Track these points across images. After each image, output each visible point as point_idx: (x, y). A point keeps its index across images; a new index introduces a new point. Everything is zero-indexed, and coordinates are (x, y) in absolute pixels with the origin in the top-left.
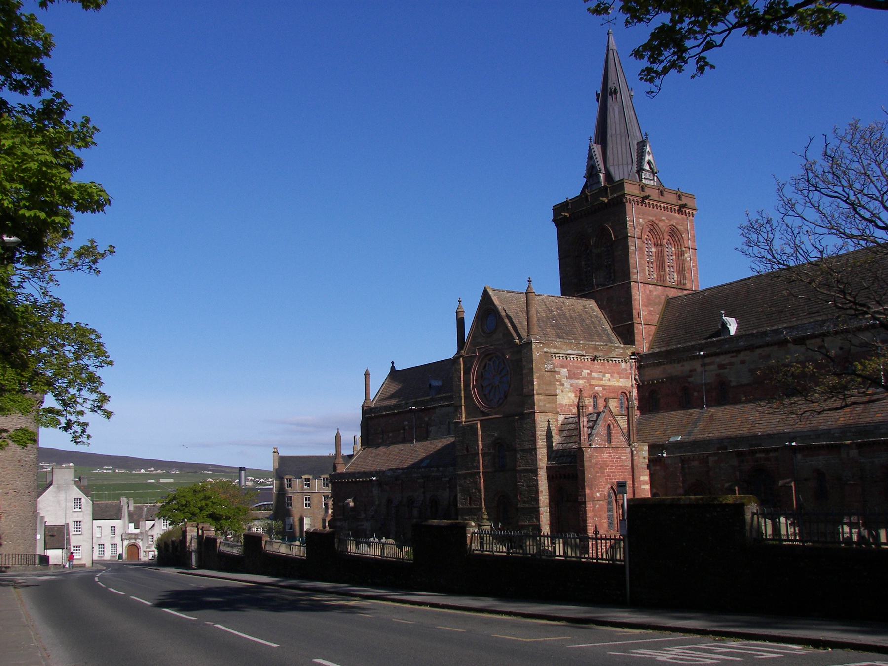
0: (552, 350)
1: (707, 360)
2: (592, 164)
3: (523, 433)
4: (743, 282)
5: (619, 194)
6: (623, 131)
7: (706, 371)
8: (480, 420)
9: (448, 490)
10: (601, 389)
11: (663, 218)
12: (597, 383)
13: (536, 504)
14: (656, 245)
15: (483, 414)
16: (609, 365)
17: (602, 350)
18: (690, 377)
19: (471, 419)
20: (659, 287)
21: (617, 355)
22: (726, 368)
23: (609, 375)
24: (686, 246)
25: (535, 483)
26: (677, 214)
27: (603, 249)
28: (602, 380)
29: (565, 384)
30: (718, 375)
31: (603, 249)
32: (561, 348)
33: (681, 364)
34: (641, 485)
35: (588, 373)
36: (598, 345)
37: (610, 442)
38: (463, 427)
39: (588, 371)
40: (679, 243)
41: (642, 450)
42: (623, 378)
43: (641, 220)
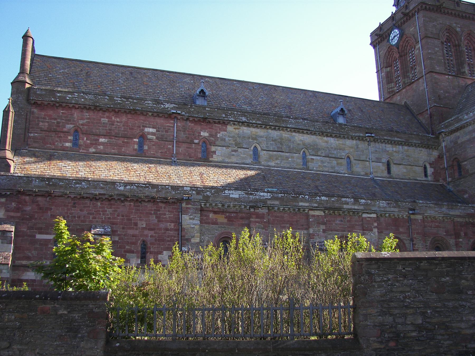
9: (376, 230)
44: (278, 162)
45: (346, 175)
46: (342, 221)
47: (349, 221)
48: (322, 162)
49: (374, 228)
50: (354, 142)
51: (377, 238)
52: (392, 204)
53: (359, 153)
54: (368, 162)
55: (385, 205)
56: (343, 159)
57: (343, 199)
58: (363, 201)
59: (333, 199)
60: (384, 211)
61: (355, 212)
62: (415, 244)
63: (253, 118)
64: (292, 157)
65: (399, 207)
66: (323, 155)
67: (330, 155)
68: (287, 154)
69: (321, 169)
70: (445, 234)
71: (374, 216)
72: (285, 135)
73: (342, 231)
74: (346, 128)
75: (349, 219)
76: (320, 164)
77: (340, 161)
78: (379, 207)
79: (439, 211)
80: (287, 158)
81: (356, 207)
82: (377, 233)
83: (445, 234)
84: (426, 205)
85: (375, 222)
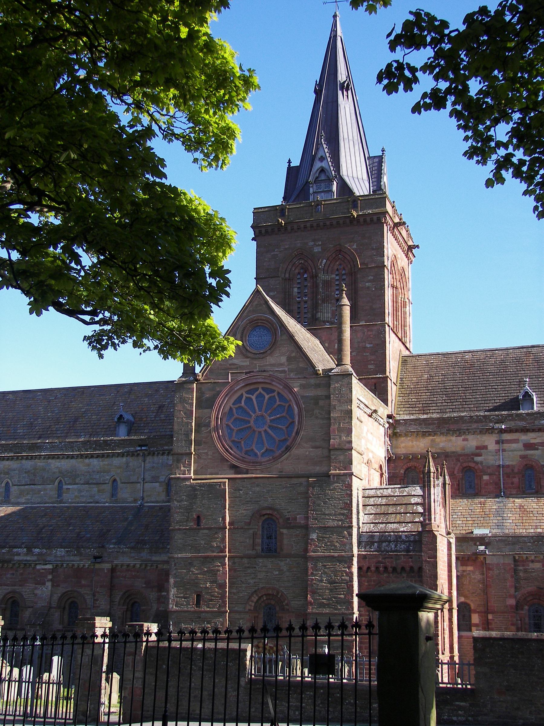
1: (506, 436)
2: (322, 167)
3: (325, 503)
4: (525, 350)
5: (377, 211)
6: (356, 138)
7: (504, 450)
8: (229, 479)
9: (49, 584)
13: (347, 609)
15: (235, 469)
18: (479, 455)
19: (208, 476)
22: (537, 449)
25: (347, 578)
27: (334, 276)
30: (523, 457)
31: (334, 276)
33: (463, 437)
38: (192, 487)
44: (29, 497)
45: (107, 504)
46: (13, 574)
47: (22, 574)
48: (80, 491)
49: (48, 581)
50: (124, 459)
51: (49, 593)
52: (72, 551)
53: (129, 473)
54: (139, 484)
55: (63, 553)
56: (106, 483)
57: (15, 550)
58: (37, 550)
59: (3, 551)
60: (60, 561)
61: (26, 565)
62: (97, 600)
63: (5, 450)
64: (45, 490)
65: (80, 554)
66: (82, 482)
67: (91, 481)
68: (39, 487)
69: (77, 500)
70: (144, 586)
71: (50, 567)
72: (40, 463)
73: (12, 585)
74: (113, 443)
75: (22, 571)
76: (76, 494)
77: (103, 487)
78: (56, 556)
79: (136, 557)
80: (40, 491)
81: (28, 558)
82: (50, 588)
83: (144, 586)
84: (118, 550)
85: (49, 574)
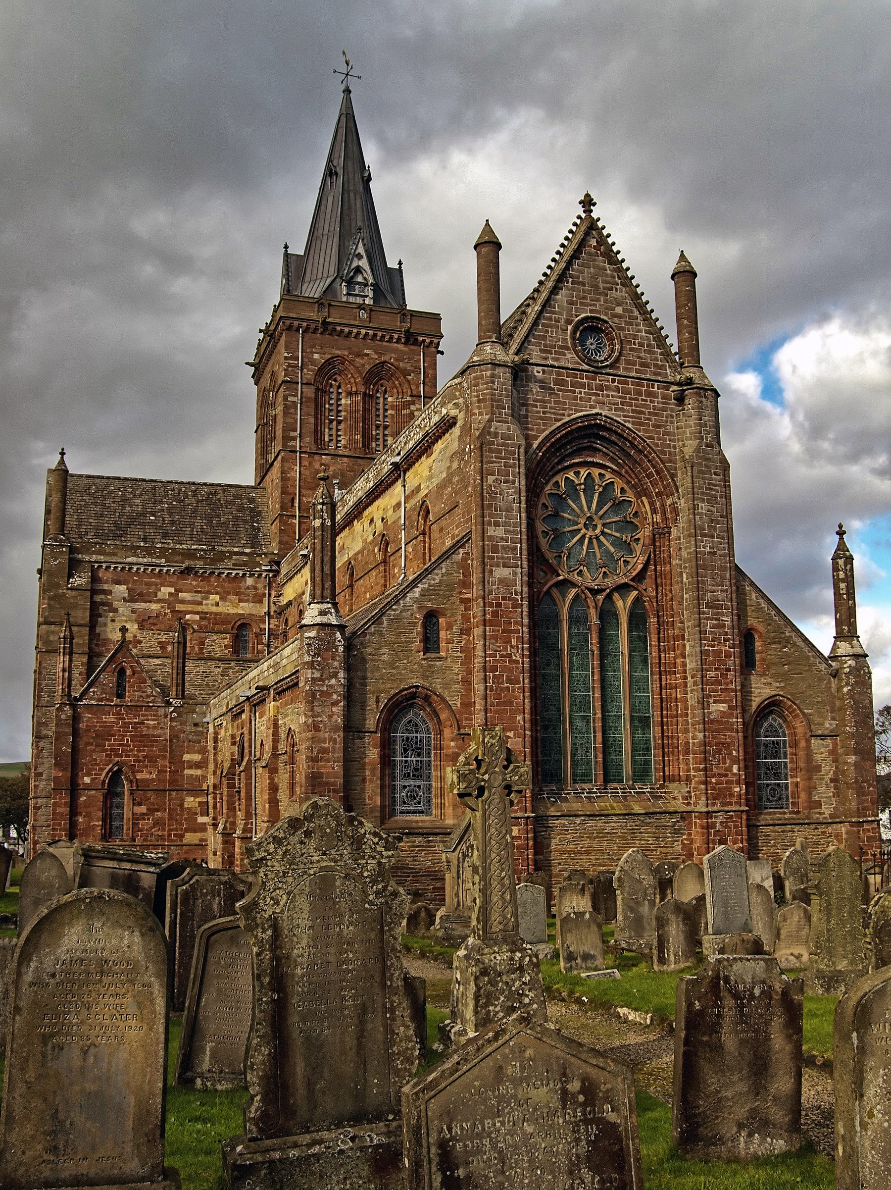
0: (94, 558)
10: (197, 617)
11: (366, 351)
12: (190, 609)
14: (350, 394)
16: (218, 581)
17: (201, 557)
20: (345, 459)
21: (234, 565)
23: (218, 597)
24: (414, 393)
26: (401, 347)
28: (200, 603)
29: (121, 610)
32: (115, 555)
34: (182, 771)
35: (170, 594)
36: (196, 550)
37: (120, 696)
39: (172, 590)
40: (400, 390)
41: (194, 712)
42: (247, 601)
43: (316, 356)
